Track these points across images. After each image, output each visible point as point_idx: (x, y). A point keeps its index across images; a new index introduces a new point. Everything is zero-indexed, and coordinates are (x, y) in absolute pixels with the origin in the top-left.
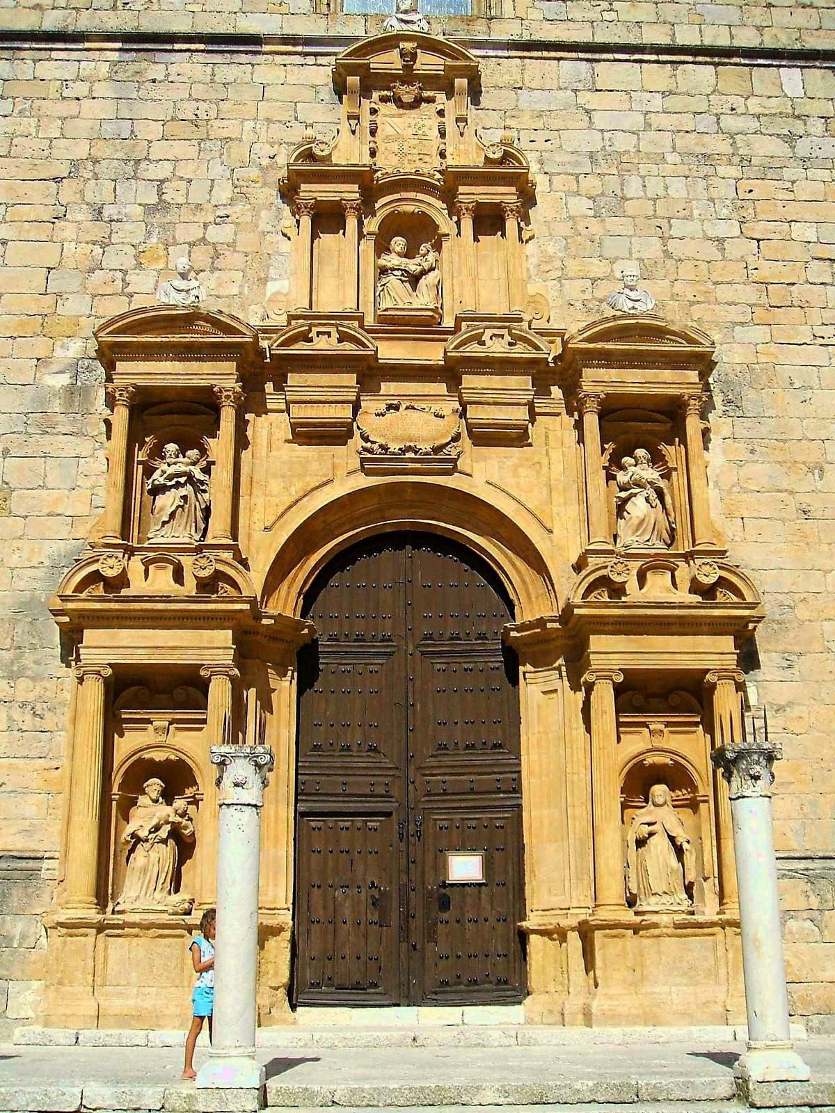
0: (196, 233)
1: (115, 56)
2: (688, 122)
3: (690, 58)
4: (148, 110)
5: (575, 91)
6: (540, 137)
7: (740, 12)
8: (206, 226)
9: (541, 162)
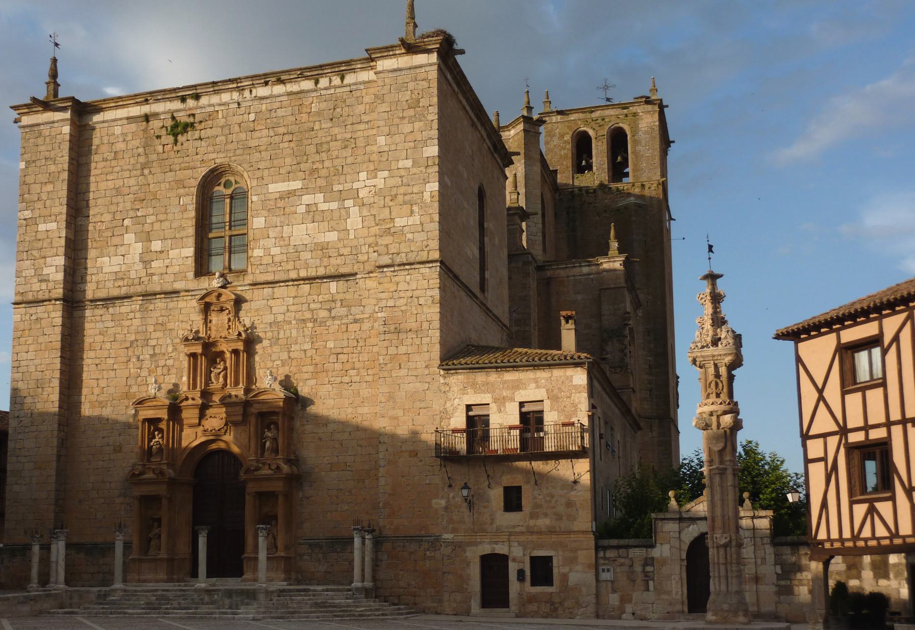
1: (140, 302)
2: (298, 307)
3: (302, 282)
4: (150, 321)
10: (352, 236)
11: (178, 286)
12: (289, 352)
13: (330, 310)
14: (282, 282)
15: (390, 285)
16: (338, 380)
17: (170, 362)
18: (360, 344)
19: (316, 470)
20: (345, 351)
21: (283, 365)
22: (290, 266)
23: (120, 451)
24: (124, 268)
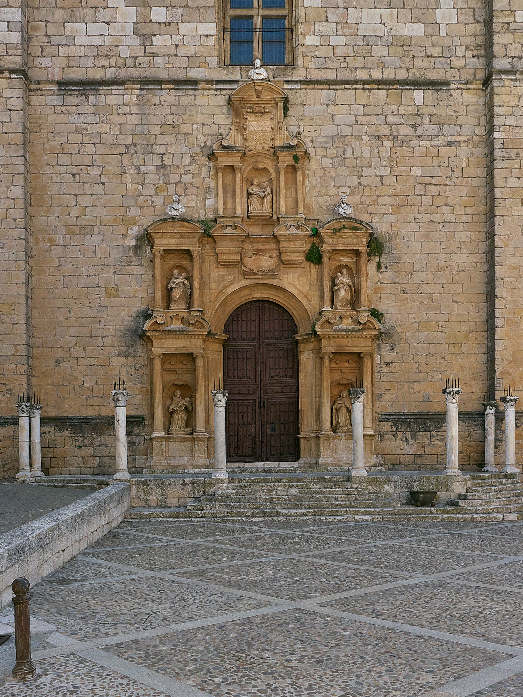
0: (177, 178)
1: (137, 92)
4: (154, 119)
5: (327, 105)
6: (312, 129)
7: (400, 61)
8: (181, 175)
9: (312, 141)
10: (443, 33)
11: (193, 74)
12: (359, 177)
13: (415, 127)
14: (347, 83)
15: (509, 98)
16: (427, 218)
17: (187, 179)
18: (456, 174)
19: (399, 329)
20: (435, 181)
21: (351, 194)
22: (359, 63)
23: (116, 295)
24: (108, 41)
